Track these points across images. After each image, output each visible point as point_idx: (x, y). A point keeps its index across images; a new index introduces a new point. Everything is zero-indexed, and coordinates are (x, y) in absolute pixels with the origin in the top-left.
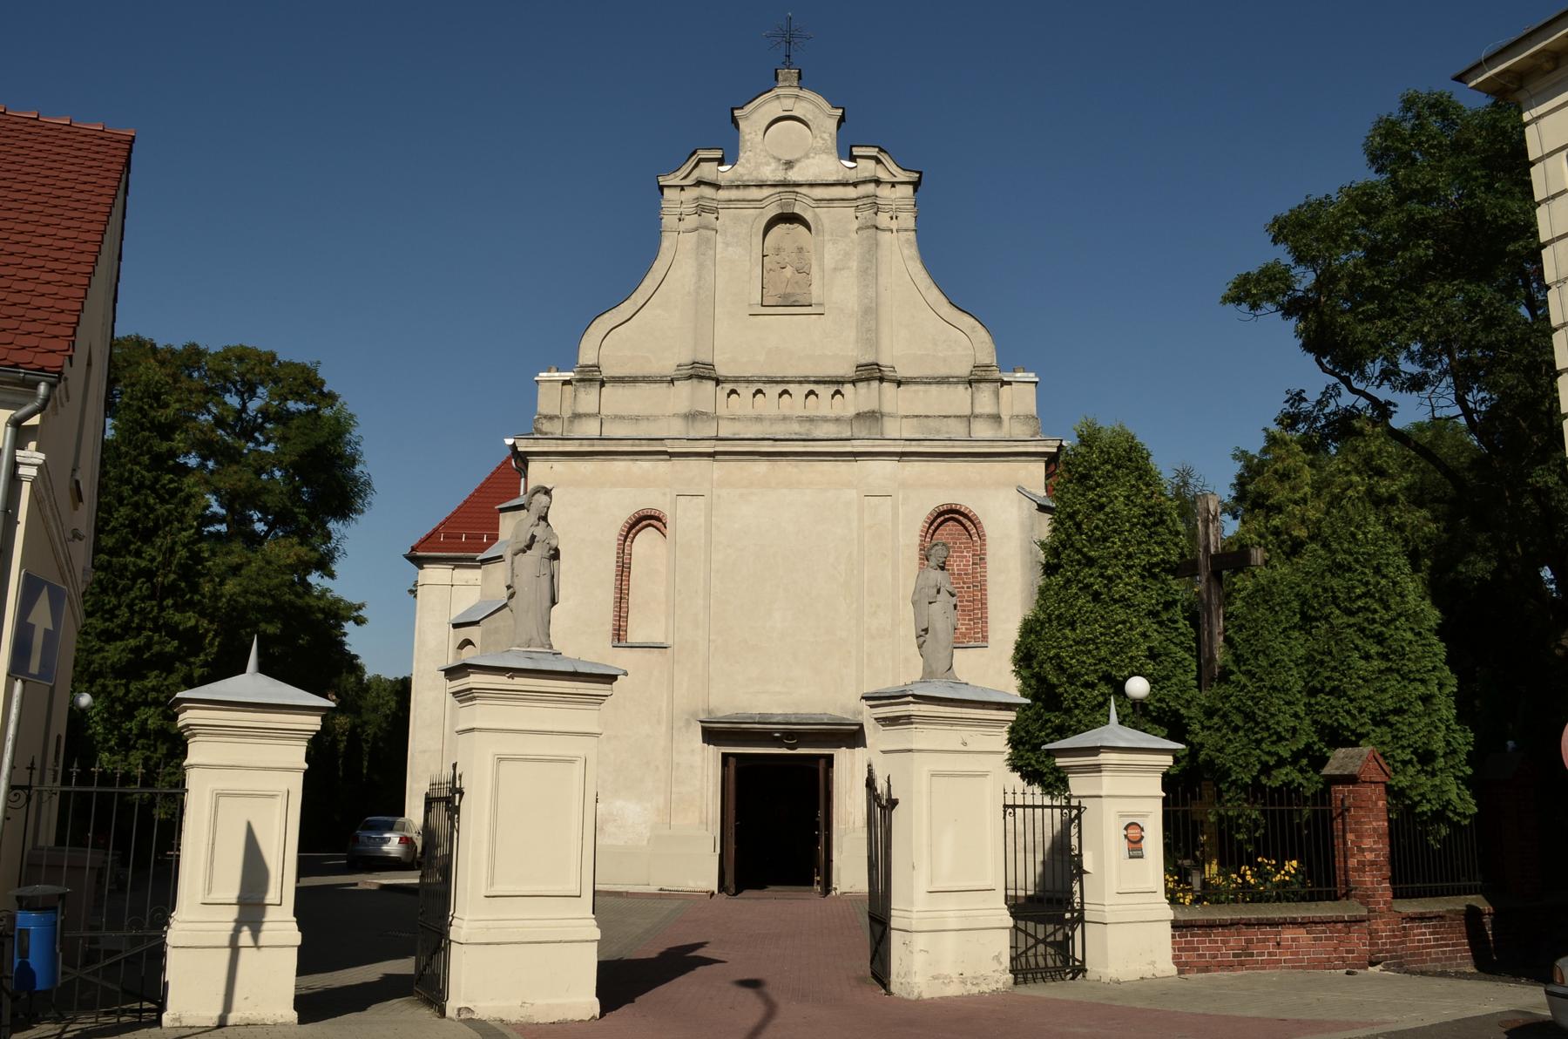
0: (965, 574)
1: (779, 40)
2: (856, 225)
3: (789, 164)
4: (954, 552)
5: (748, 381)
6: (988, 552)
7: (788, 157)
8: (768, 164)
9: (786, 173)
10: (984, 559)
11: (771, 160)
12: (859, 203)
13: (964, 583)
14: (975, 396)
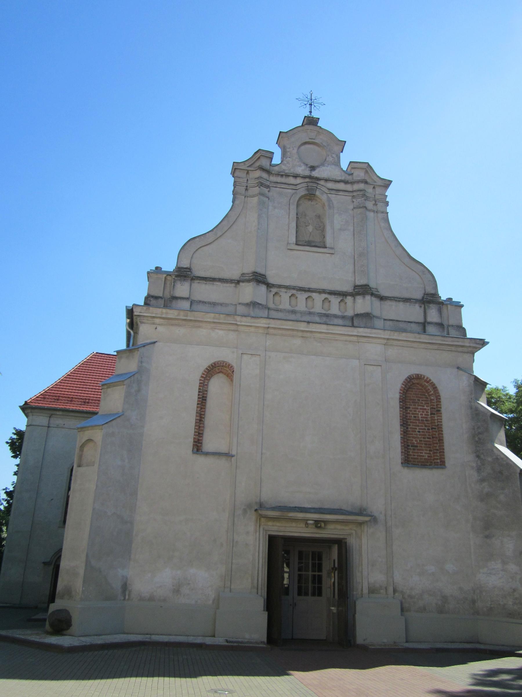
0: (426, 421)
1: (306, 103)
2: (351, 207)
3: (313, 168)
4: (418, 406)
5: (287, 287)
6: (442, 406)
7: (312, 164)
8: (300, 166)
9: (311, 173)
10: (439, 411)
11: (302, 164)
12: (355, 194)
13: (426, 426)
14: (427, 311)
